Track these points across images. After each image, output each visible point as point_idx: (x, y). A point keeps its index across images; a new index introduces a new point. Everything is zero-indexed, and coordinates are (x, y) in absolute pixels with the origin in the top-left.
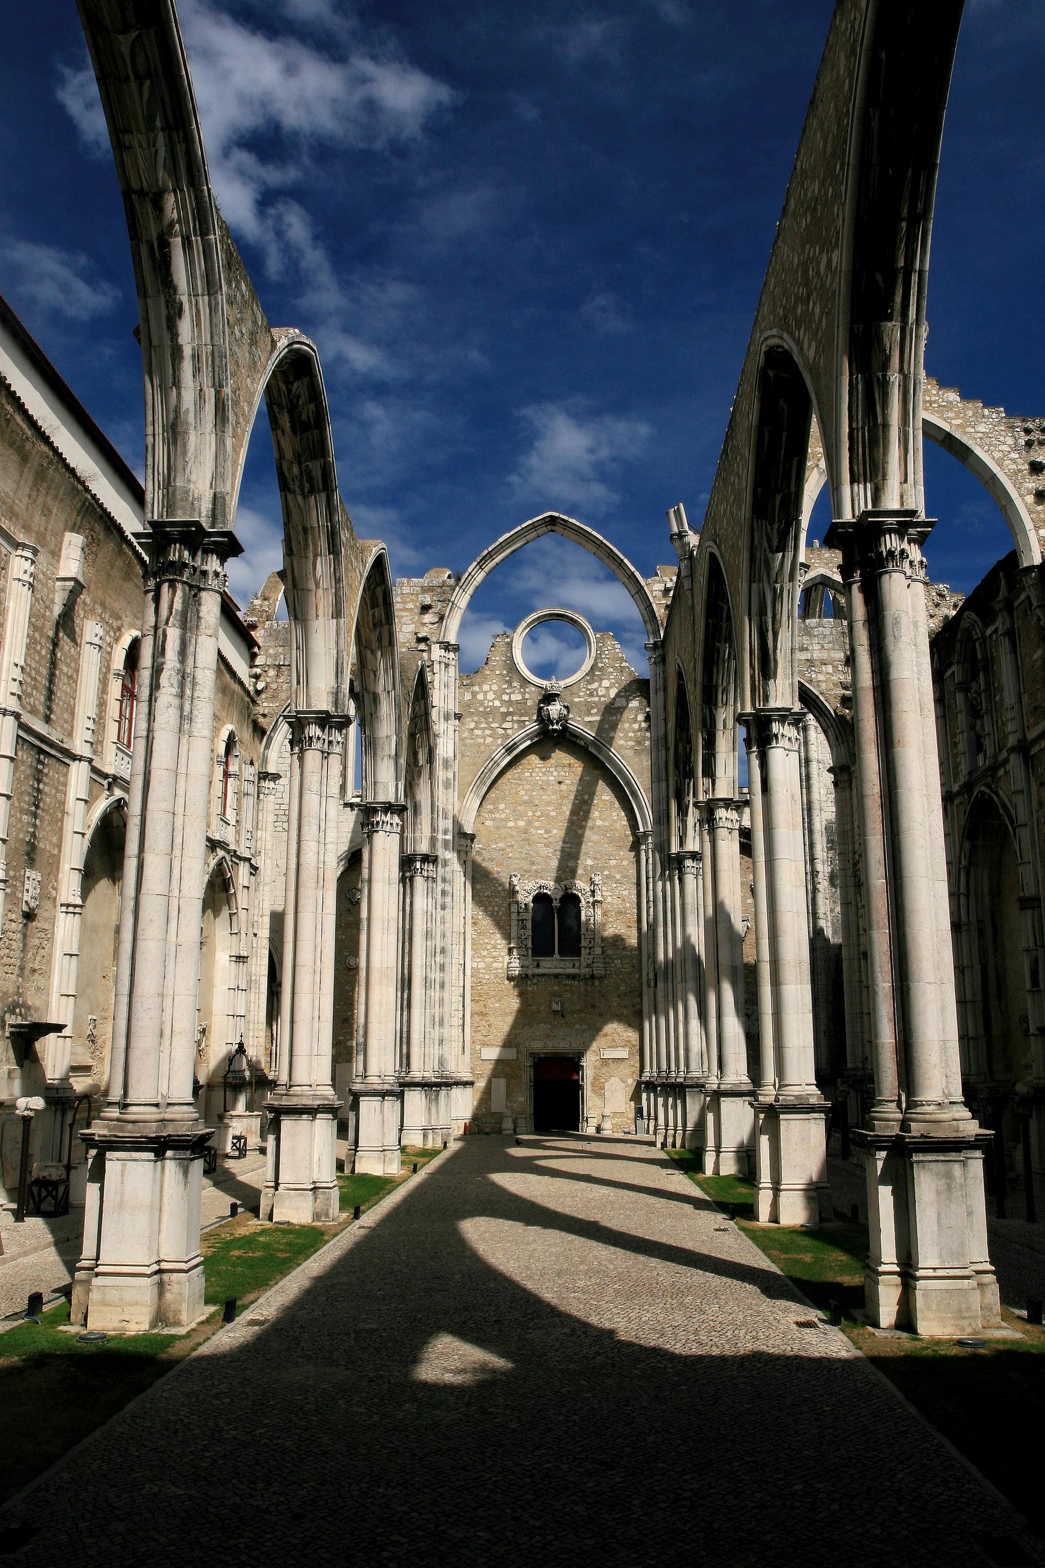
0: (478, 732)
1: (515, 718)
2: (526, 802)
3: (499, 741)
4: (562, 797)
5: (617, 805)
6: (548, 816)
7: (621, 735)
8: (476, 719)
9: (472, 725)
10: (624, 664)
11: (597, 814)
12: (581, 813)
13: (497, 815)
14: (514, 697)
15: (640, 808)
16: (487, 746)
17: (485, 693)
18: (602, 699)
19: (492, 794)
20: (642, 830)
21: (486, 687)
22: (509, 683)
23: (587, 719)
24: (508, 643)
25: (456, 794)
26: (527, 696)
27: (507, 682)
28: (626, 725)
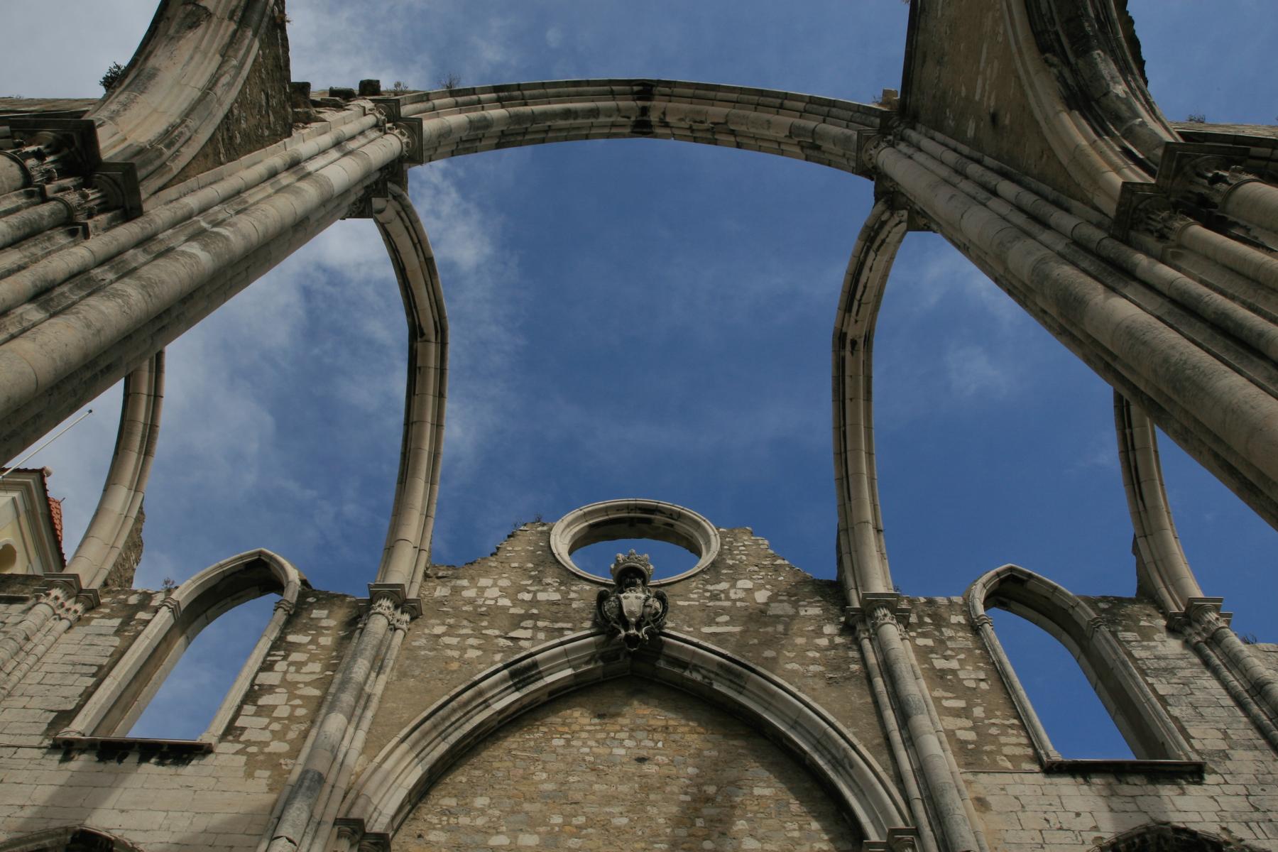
0: (447, 640)
1: (540, 624)
2: (545, 797)
3: (498, 657)
4: (646, 788)
5: (795, 806)
6: (605, 826)
7: (792, 655)
8: (452, 621)
9: (439, 630)
10: (779, 562)
11: (741, 825)
12: (700, 823)
13: (464, 820)
14: (542, 596)
15: (863, 791)
16: (469, 662)
17: (482, 590)
18: (738, 604)
19: (460, 777)
20: (873, 836)
21: (483, 582)
22: (538, 580)
23: (706, 630)
24: (542, 532)
25: (361, 735)
26: (572, 595)
27: (531, 577)
28: (800, 641)
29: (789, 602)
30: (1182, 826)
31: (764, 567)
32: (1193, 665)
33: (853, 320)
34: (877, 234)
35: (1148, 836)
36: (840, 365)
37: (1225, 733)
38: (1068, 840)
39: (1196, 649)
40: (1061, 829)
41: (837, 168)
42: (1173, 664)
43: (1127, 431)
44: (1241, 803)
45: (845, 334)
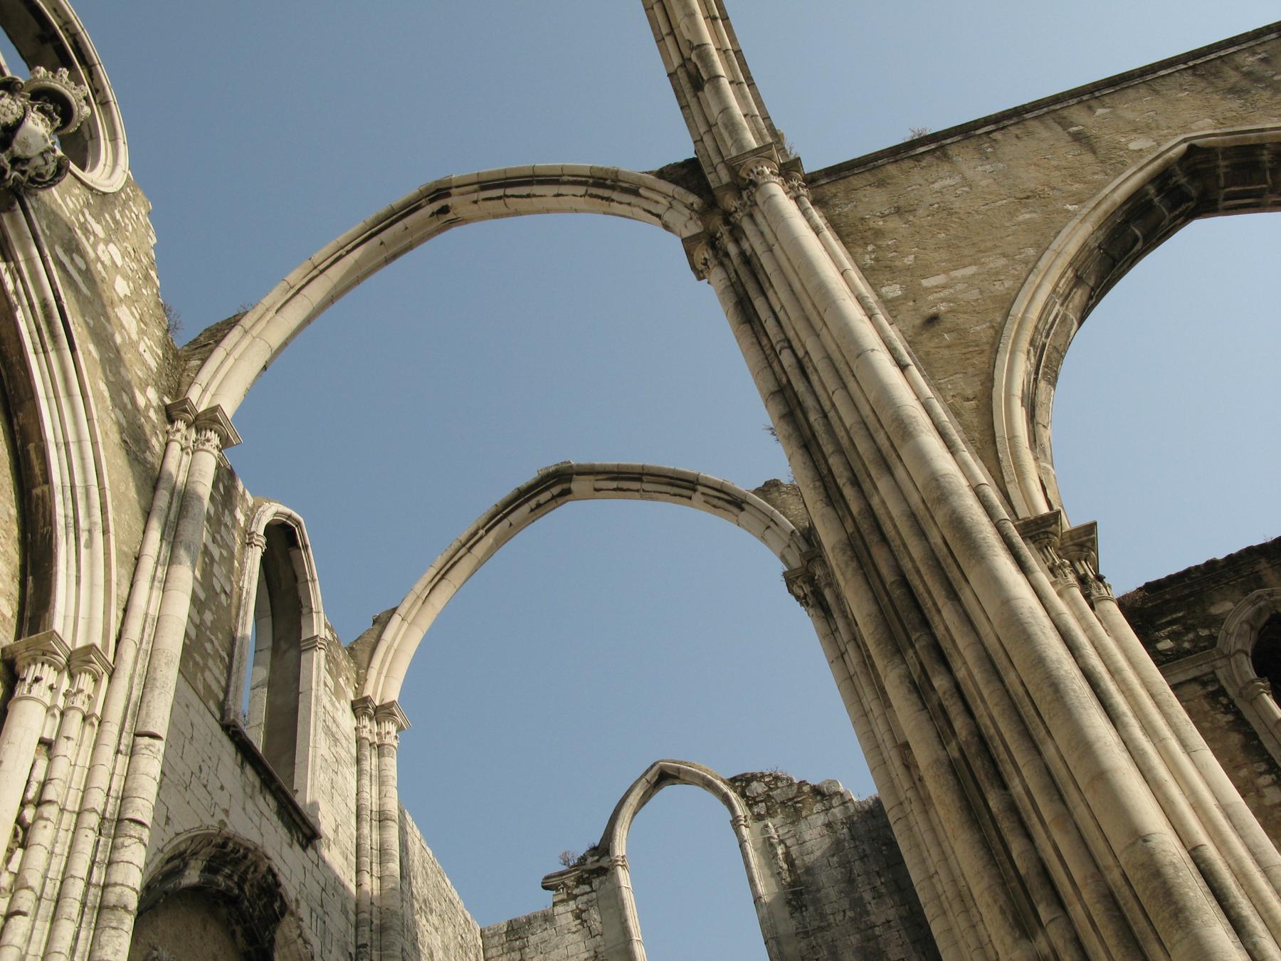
29: (138, 326)
30: (276, 870)
31: (140, 261)
32: (349, 752)
33: (475, 197)
34: (613, 188)
35: (250, 856)
36: (410, 208)
37: (337, 827)
38: (204, 802)
39: (359, 741)
40: (205, 786)
41: (686, 119)
42: (339, 736)
43: (482, 532)
44: (316, 891)
45: (449, 195)
